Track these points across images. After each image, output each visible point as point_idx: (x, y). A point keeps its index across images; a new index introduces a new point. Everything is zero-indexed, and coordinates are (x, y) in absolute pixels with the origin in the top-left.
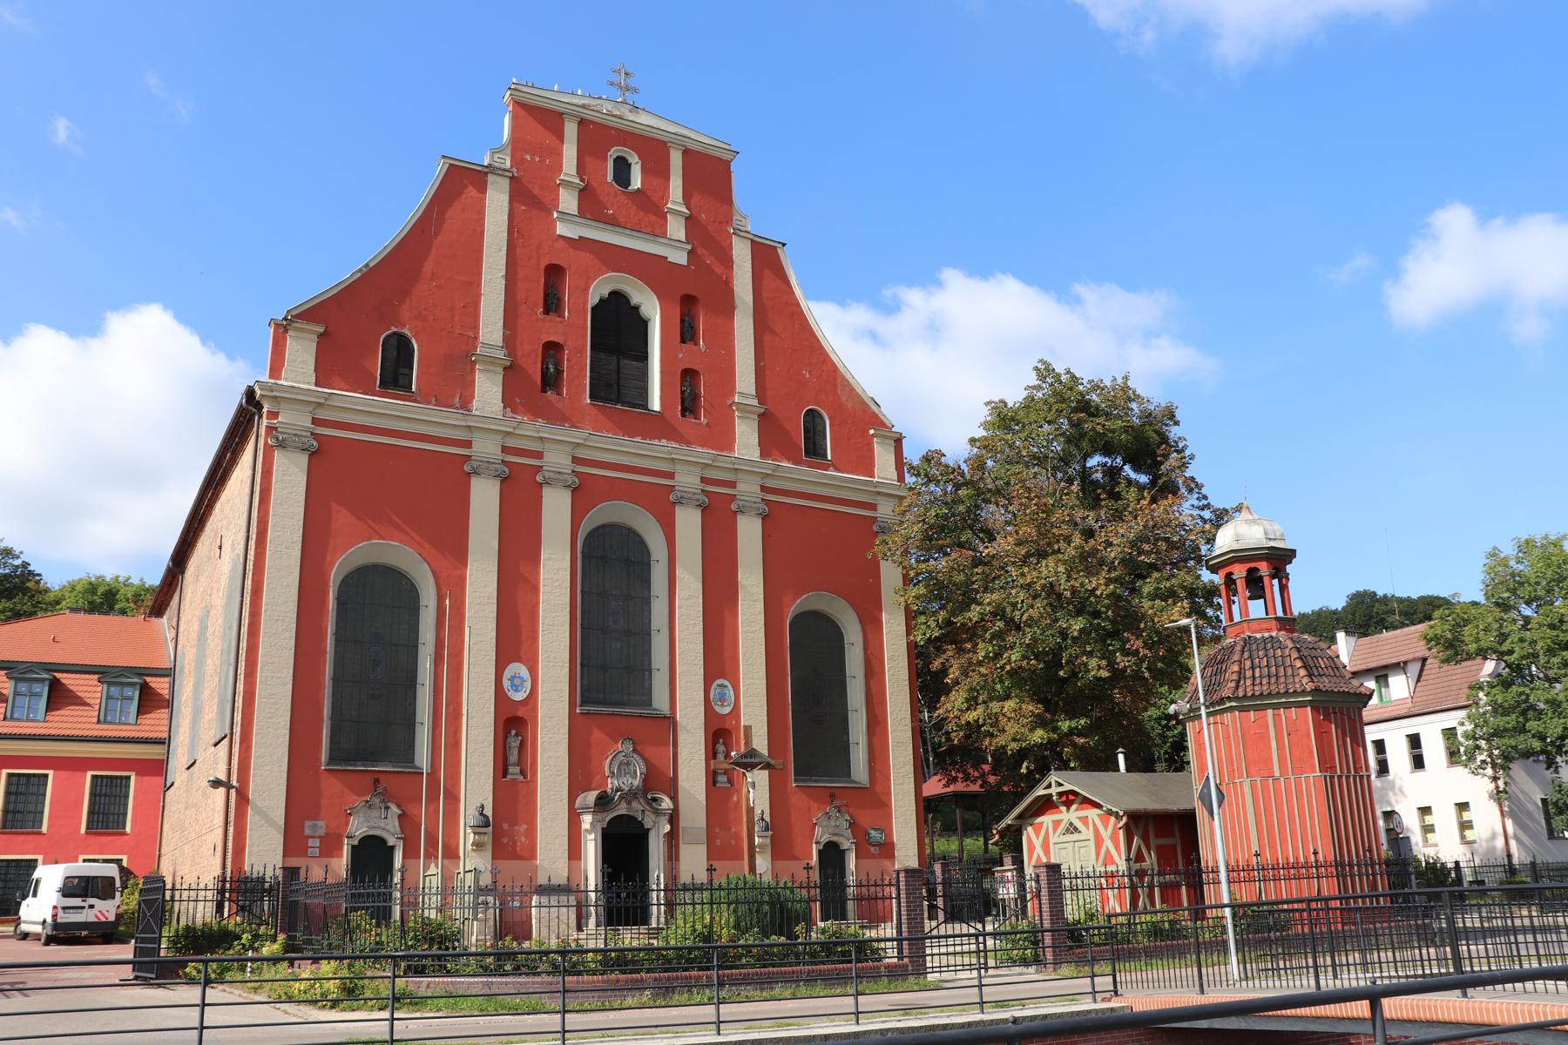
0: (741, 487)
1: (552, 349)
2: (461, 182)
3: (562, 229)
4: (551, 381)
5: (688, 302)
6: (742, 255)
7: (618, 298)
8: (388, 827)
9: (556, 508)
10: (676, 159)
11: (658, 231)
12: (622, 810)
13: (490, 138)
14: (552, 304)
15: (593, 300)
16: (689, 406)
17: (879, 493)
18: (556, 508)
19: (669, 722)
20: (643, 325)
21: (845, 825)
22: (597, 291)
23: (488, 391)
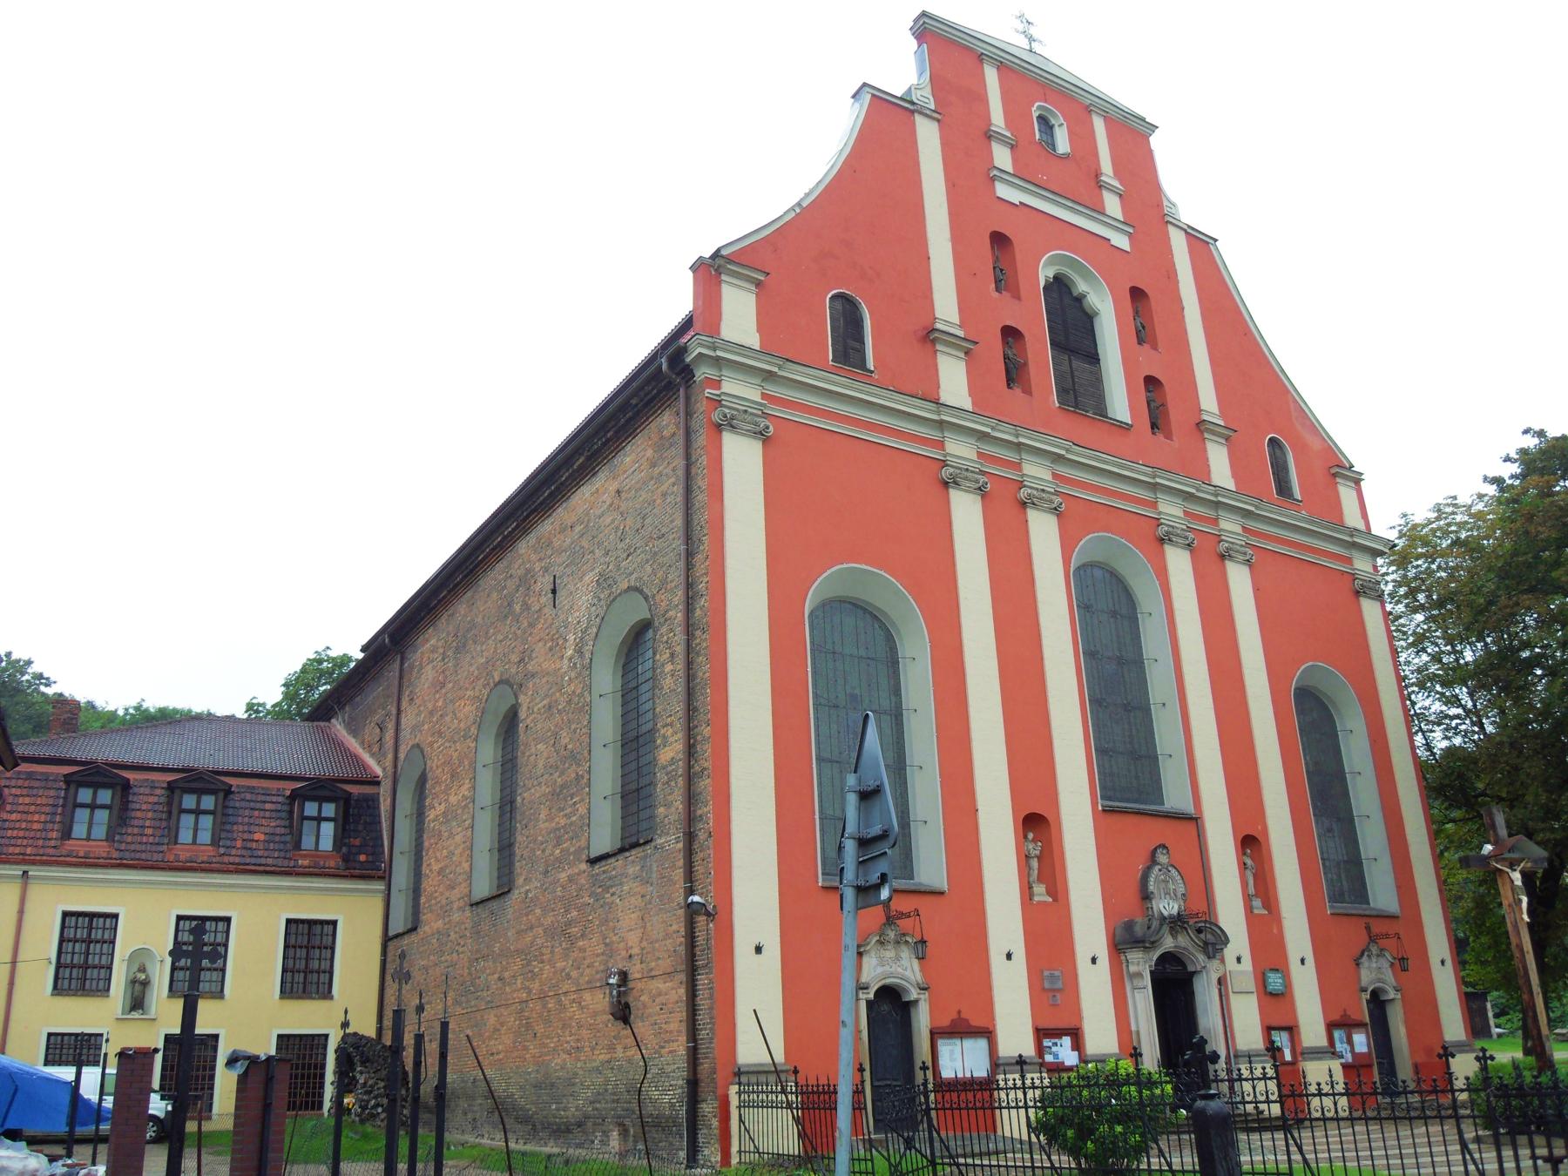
0: (1224, 525)
1: (1011, 334)
2: (885, 115)
3: (1003, 191)
4: (1015, 373)
5: (1137, 294)
6: (1178, 242)
7: (1059, 287)
8: (904, 969)
9: (1043, 531)
10: (1099, 125)
11: (1098, 210)
12: (1168, 943)
13: (901, 71)
14: (1004, 279)
15: (1042, 284)
16: (1158, 421)
17: (1354, 545)
18: (1043, 531)
19: (1193, 820)
20: (1087, 320)
21: (1387, 965)
22: (1045, 273)
23: (953, 381)
